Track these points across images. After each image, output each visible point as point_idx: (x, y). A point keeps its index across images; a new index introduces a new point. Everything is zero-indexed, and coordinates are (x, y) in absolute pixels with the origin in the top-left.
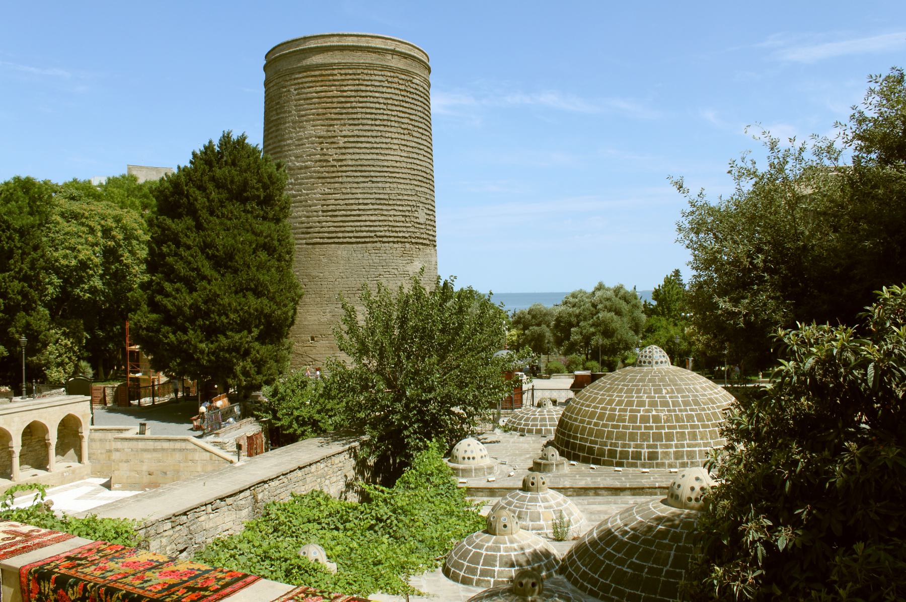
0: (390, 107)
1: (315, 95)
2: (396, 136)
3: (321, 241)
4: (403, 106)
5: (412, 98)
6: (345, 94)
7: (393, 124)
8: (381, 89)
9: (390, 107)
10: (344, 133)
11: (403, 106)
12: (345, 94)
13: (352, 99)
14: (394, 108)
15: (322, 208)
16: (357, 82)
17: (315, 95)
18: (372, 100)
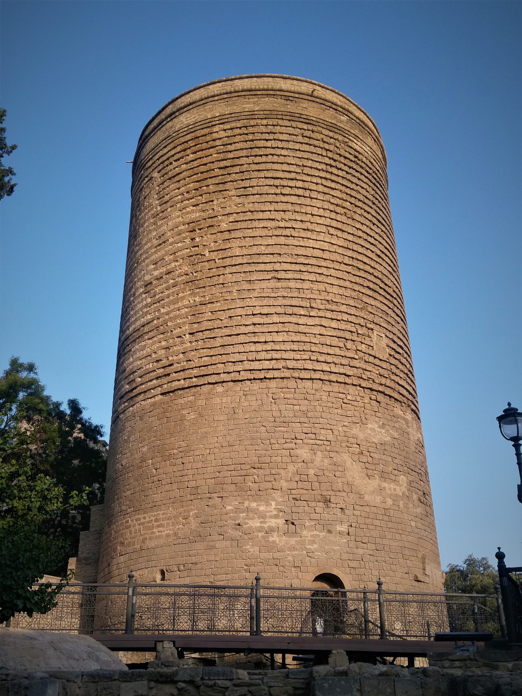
0: (307, 170)
1: (184, 167)
2: (321, 212)
3: (187, 384)
4: (331, 173)
5: (350, 167)
6: (231, 155)
7: (314, 195)
8: (291, 145)
9: (307, 170)
10: (228, 210)
11: (331, 173)
12: (231, 155)
13: (243, 161)
14: (317, 173)
15: (188, 331)
16: (251, 137)
17: (184, 167)
18: (275, 159)
